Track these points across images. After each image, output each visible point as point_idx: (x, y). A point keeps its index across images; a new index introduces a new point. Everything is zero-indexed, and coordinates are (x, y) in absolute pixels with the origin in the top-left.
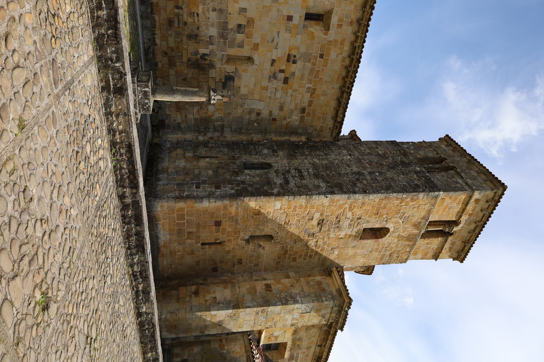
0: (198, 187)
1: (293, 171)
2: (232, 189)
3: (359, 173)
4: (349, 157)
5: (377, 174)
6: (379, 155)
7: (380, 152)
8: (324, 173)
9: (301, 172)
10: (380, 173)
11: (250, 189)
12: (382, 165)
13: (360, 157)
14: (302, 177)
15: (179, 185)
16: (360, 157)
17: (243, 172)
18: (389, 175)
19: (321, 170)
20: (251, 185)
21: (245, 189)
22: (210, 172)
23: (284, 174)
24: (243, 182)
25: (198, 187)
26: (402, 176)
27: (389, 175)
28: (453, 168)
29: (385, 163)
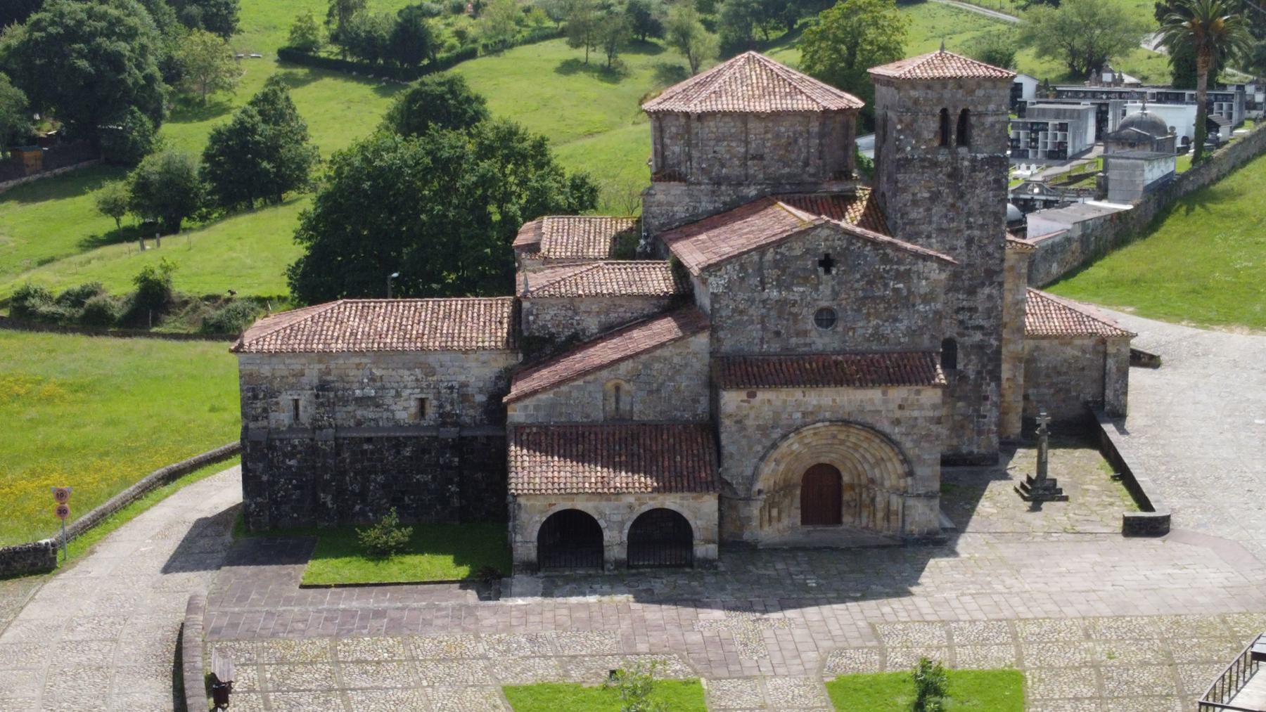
0: (985, 417)
1: (961, 317)
2: (989, 385)
3: (970, 241)
4: (934, 240)
5: (971, 220)
6: (930, 198)
7: (927, 195)
8: (966, 283)
9: (963, 308)
10: (969, 214)
11: (989, 368)
12: (953, 205)
13: (934, 226)
14: (972, 310)
15: (980, 433)
16: (934, 226)
17: (961, 371)
18: (974, 205)
19: (960, 284)
20: (984, 366)
21: (990, 372)
22: (960, 404)
23: (967, 328)
24: (979, 373)
25: (985, 417)
26: (978, 191)
27: (974, 205)
28: (965, 113)
29: (950, 200)
